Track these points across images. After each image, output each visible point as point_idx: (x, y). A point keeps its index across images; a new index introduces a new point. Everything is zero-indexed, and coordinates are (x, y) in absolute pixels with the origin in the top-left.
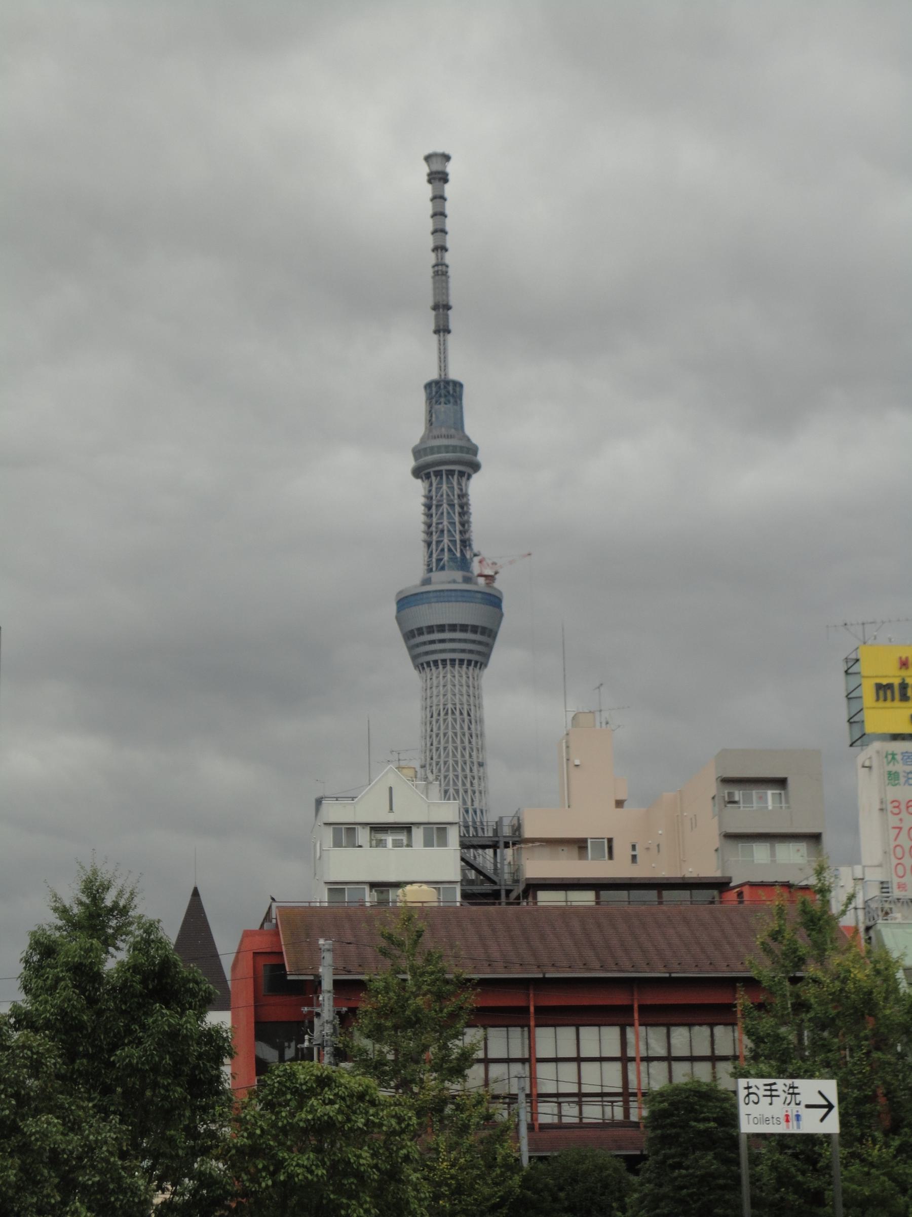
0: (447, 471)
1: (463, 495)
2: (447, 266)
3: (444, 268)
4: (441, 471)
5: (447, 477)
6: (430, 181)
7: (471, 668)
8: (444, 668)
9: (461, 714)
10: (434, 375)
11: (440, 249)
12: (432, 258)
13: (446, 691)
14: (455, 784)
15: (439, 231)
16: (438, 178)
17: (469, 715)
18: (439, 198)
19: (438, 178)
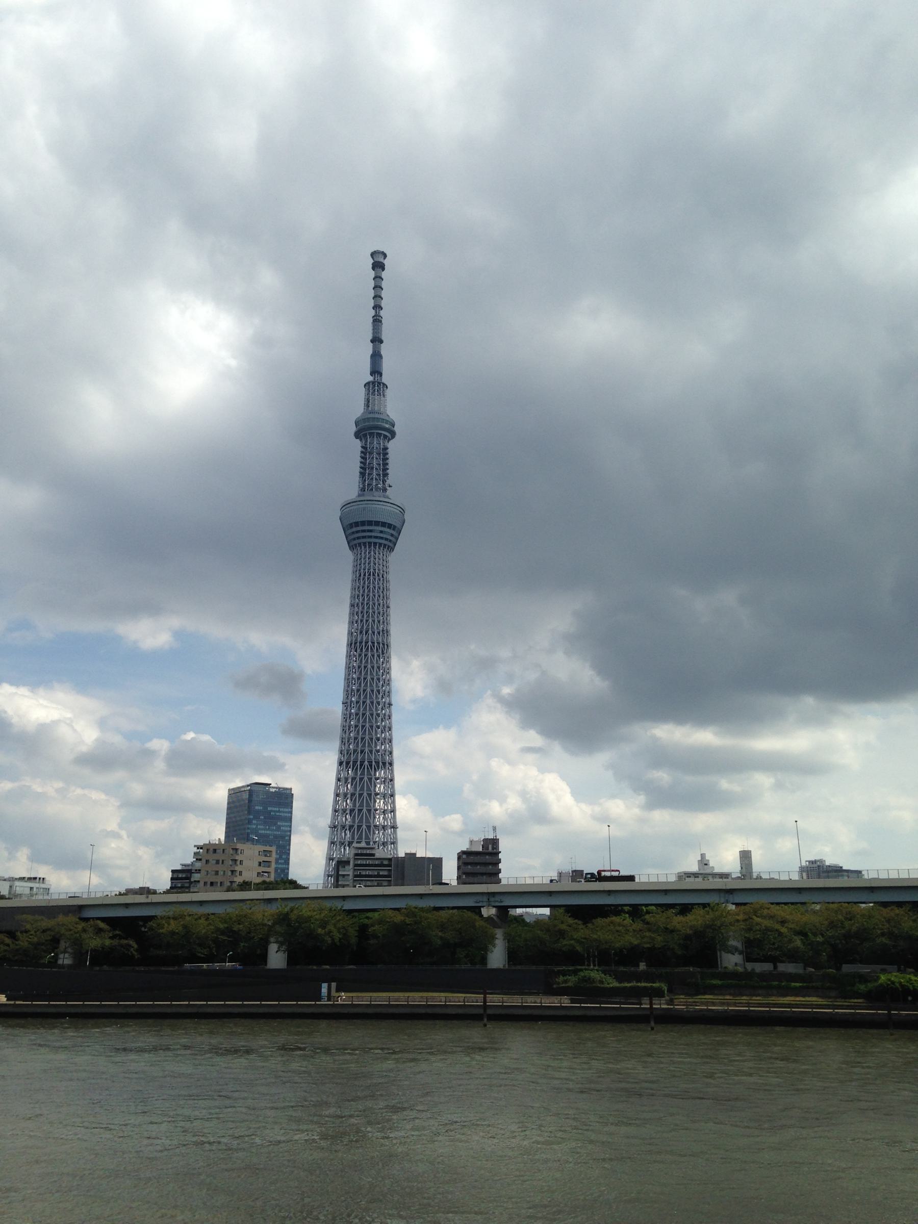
0: (376, 433)
1: (386, 449)
2: (382, 318)
3: (380, 318)
4: (374, 433)
5: (377, 437)
6: (373, 268)
7: (385, 550)
8: (369, 547)
9: (378, 575)
10: (371, 379)
11: (377, 307)
12: (373, 313)
13: (370, 561)
14: (372, 616)
15: (377, 297)
16: (378, 266)
17: (383, 577)
18: (378, 278)
19: (378, 266)
